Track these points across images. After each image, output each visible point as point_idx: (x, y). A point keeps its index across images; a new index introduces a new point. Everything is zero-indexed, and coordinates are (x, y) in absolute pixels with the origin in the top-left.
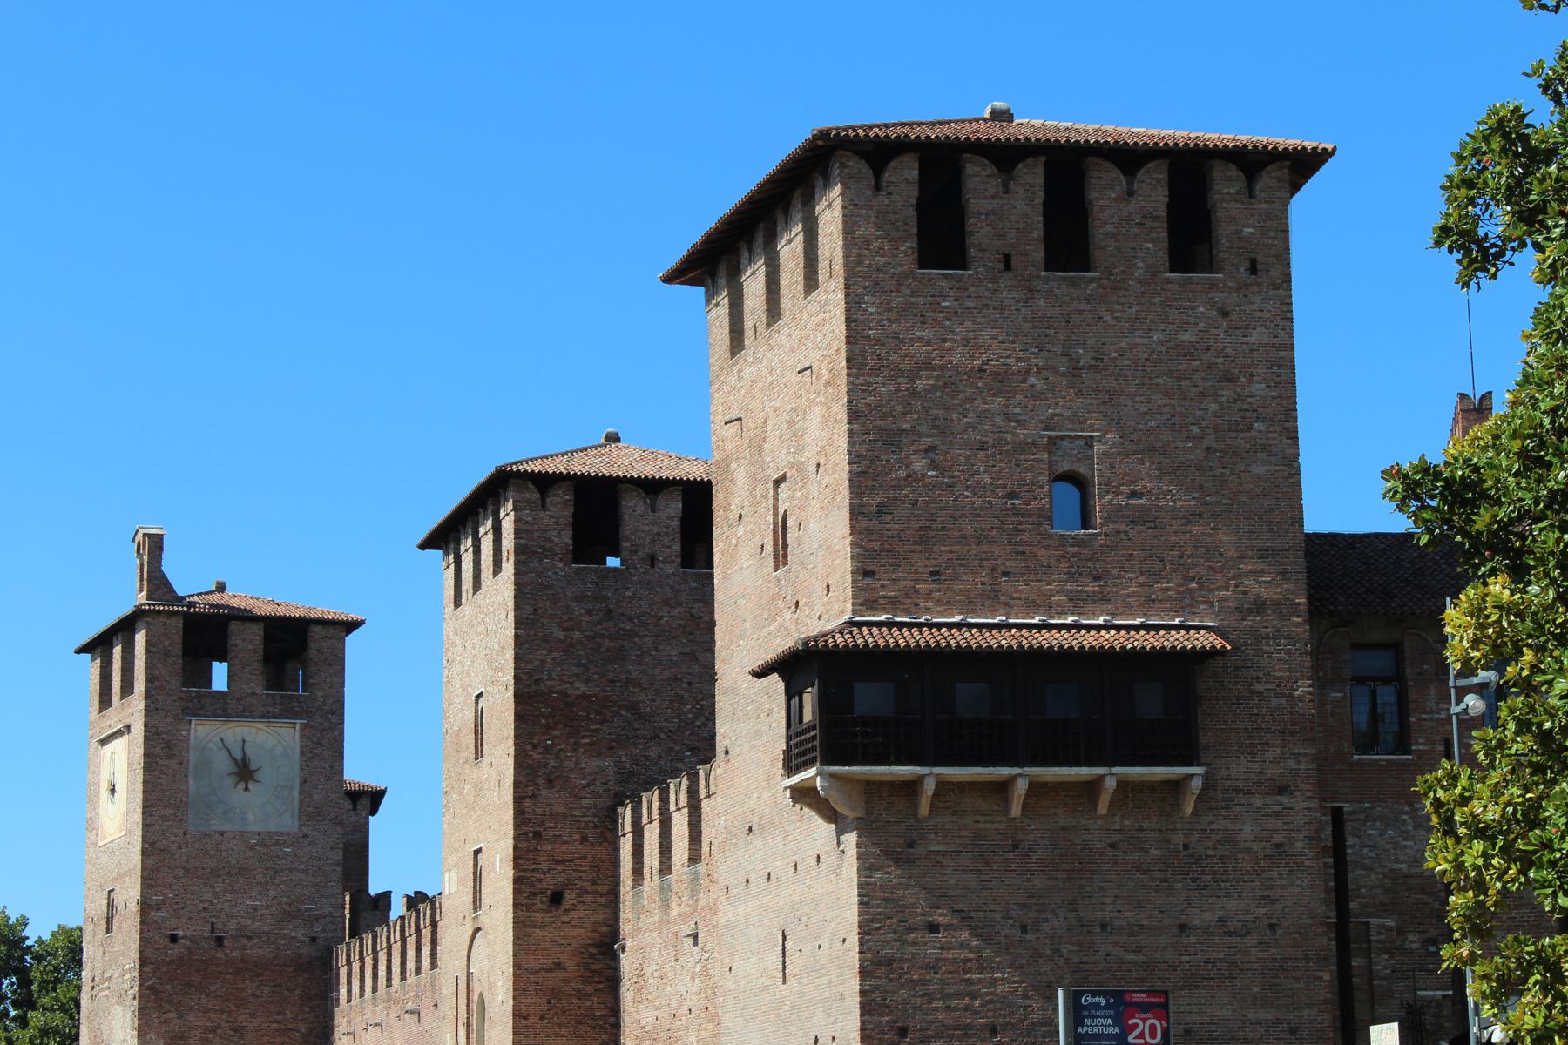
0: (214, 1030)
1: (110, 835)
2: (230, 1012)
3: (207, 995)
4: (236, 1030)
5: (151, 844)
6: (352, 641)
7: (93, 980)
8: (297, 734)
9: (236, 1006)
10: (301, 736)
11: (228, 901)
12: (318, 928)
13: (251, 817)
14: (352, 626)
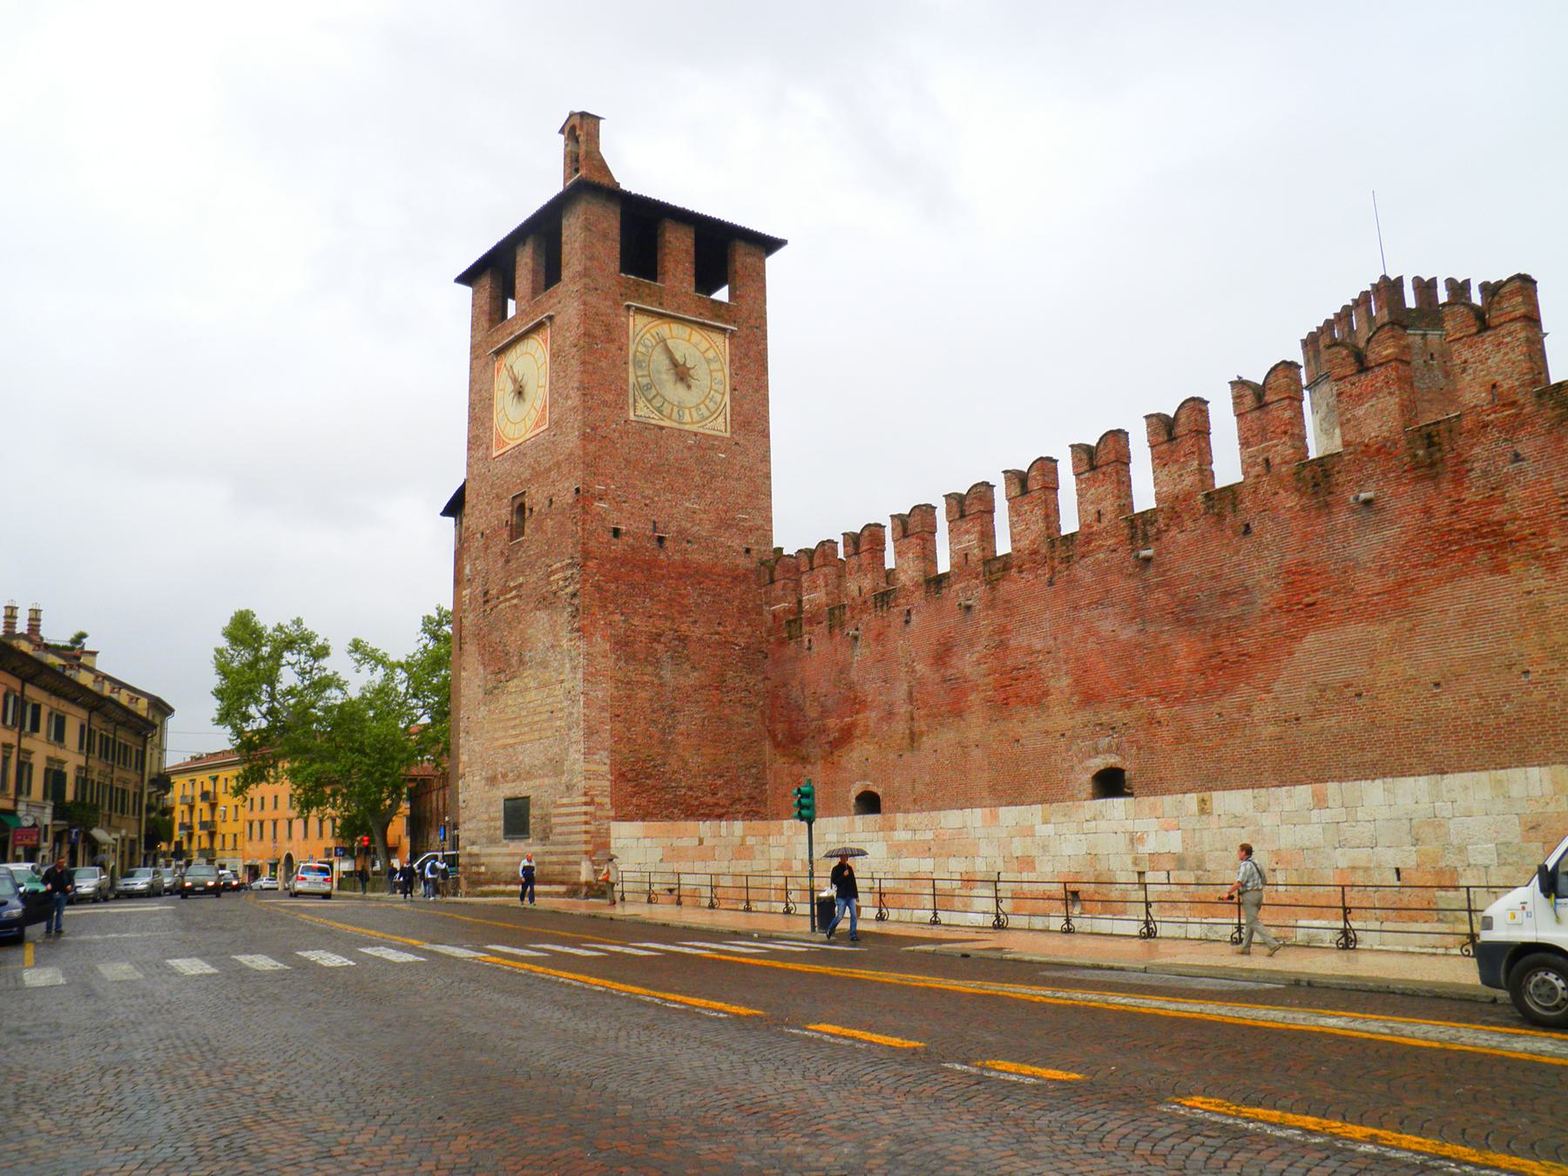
0: (657, 637)
1: (513, 439)
2: (673, 620)
3: (651, 599)
4: (679, 638)
5: (592, 429)
6: (773, 262)
7: (486, 593)
8: (727, 341)
9: (680, 613)
10: (730, 344)
11: (668, 500)
12: (752, 539)
13: (687, 418)
14: (770, 245)
